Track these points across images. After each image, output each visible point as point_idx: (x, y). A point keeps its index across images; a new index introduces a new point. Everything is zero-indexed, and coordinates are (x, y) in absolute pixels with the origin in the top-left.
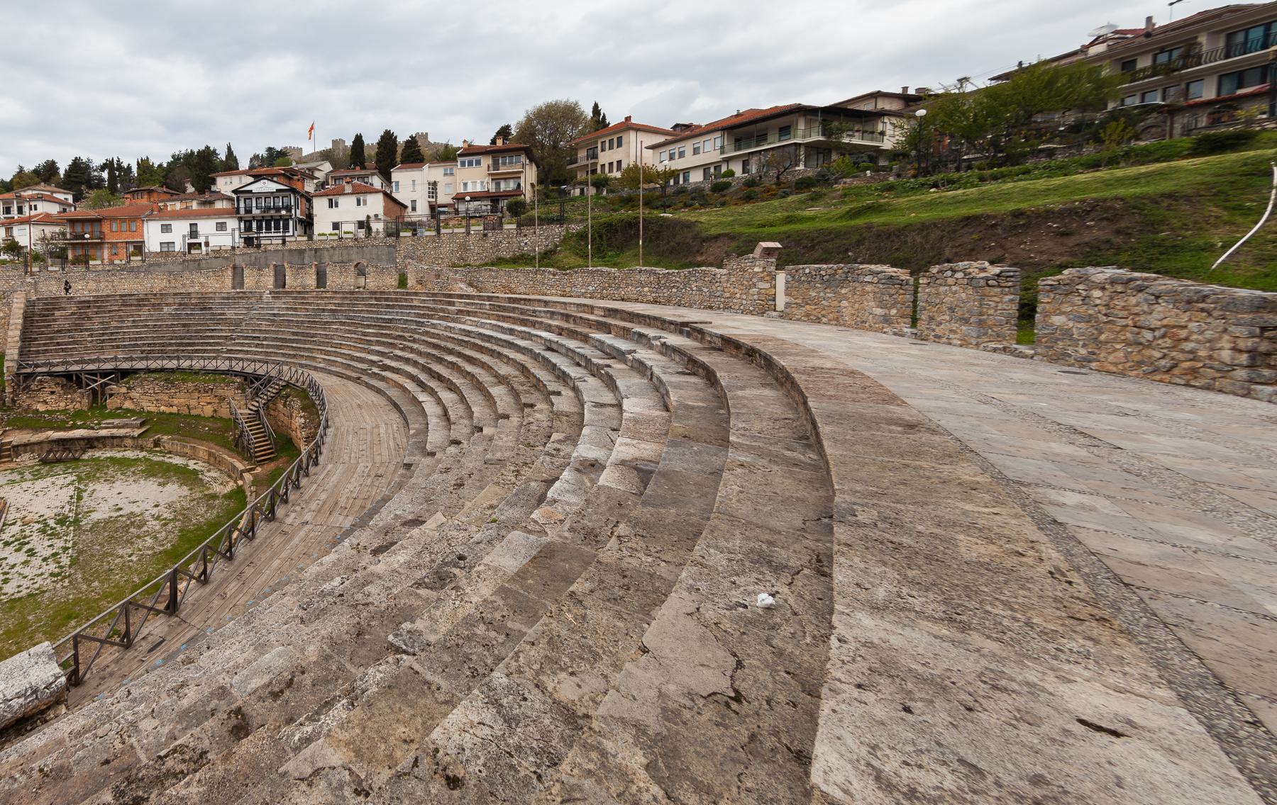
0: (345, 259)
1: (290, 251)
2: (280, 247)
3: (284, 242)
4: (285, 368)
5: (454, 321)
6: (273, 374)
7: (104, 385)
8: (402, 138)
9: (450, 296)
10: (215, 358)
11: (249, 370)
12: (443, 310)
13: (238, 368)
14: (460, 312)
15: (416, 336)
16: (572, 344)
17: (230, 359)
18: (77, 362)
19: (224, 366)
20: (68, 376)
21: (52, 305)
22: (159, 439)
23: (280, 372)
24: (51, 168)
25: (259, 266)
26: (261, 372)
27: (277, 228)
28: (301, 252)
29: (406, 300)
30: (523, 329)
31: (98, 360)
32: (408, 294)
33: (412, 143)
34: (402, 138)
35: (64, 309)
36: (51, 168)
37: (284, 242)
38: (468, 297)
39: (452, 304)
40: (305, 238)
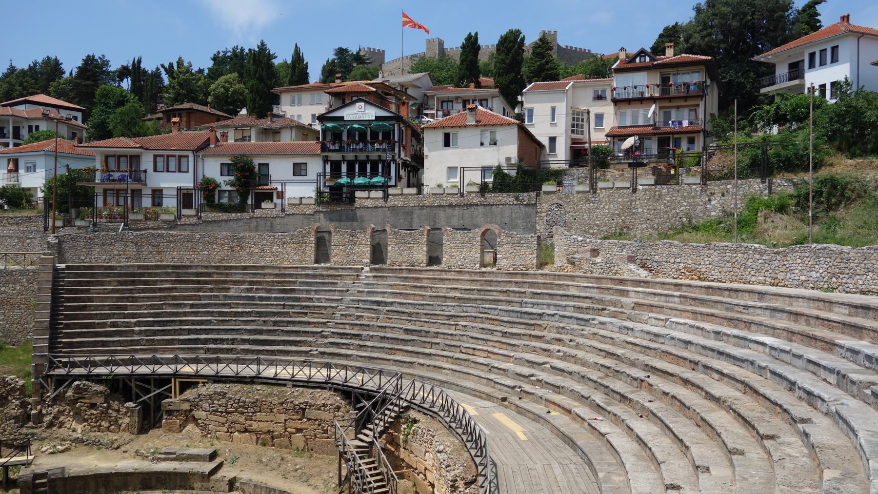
0: (467, 223)
2: (381, 203)
3: (386, 197)
5: (629, 319)
6: (390, 389)
9: (622, 282)
12: (614, 304)
15: (581, 340)
16: (812, 354)
17: (328, 366)
18: (125, 363)
19: (320, 375)
21: (89, 275)
26: (371, 385)
29: (559, 286)
30: (735, 332)
37: (386, 197)
40: (413, 191)
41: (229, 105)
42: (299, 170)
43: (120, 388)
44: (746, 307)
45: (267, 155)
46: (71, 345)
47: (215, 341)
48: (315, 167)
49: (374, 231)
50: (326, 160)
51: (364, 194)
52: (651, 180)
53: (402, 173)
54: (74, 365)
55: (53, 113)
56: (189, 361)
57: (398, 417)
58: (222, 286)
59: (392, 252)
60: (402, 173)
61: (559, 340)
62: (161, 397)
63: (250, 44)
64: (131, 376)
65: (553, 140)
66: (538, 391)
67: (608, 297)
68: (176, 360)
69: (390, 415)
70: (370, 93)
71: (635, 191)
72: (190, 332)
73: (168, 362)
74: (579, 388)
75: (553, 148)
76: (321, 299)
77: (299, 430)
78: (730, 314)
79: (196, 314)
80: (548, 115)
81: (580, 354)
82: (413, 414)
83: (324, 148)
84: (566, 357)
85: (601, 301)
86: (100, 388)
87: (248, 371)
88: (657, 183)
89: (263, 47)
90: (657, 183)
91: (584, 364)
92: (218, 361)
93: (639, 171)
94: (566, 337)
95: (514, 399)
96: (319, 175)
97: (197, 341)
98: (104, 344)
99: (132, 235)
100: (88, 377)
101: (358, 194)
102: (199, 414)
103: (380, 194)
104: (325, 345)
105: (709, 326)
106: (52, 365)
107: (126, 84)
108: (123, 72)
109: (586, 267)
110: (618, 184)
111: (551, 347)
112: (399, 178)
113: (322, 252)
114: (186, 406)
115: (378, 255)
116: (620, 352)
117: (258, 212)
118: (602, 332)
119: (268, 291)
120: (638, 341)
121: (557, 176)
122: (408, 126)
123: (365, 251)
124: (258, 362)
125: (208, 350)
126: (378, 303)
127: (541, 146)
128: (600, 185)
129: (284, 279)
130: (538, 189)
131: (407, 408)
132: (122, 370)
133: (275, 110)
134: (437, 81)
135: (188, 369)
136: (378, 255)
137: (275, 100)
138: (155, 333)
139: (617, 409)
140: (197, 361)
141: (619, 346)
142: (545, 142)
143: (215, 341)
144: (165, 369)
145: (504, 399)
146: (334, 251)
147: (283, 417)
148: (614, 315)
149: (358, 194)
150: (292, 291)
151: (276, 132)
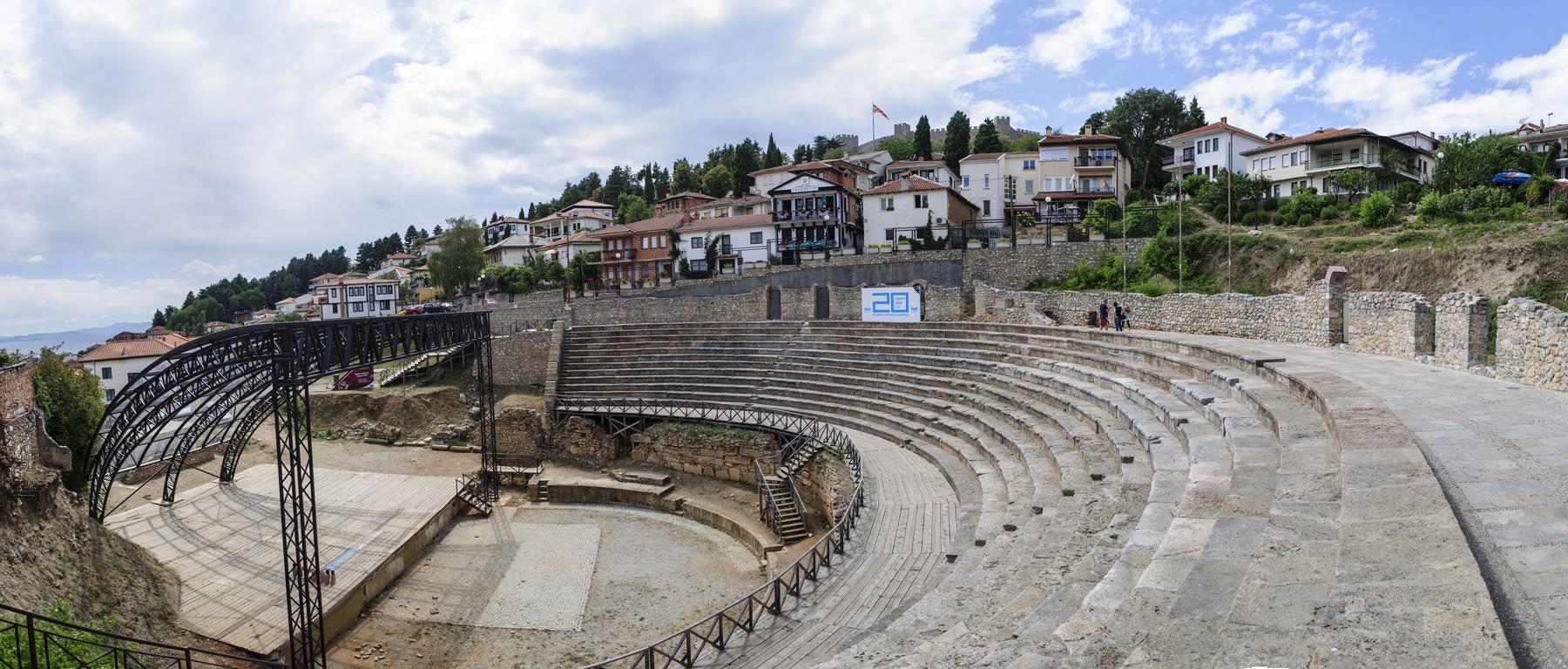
1: (835, 268)
2: (823, 264)
3: (828, 257)
4: (821, 425)
5: (1024, 364)
6: (807, 432)
7: (630, 432)
8: (976, 122)
9: (1023, 330)
10: (743, 409)
11: (780, 426)
12: (1013, 349)
13: (767, 423)
14: (1033, 351)
15: (980, 385)
17: (759, 410)
20: (596, 417)
21: (586, 335)
22: (681, 501)
23: (815, 430)
24: (594, 179)
25: (798, 286)
26: (793, 429)
27: (820, 237)
28: (847, 270)
29: (971, 335)
31: (623, 403)
32: (973, 327)
33: (988, 128)
34: (976, 122)
35: (595, 341)
36: (594, 179)
37: (828, 257)
38: (1043, 331)
39: (1024, 340)
41: (717, 189)
42: (756, 238)
43: (601, 422)
44: (1116, 350)
45: (728, 228)
46: (571, 389)
47: (676, 388)
48: (769, 234)
49: (818, 289)
50: (778, 228)
51: (808, 256)
52: (1064, 238)
53: (846, 236)
54: (570, 404)
55: (589, 213)
56: (651, 404)
57: (812, 457)
58: (684, 340)
59: (833, 306)
60: (846, 236)
61: (963, 386)
62: (630, 432)
63: (736, 142)
64: (609, 413)
65: (987, 203)
66: (938, 434)
67: (1009, 344)
68: (641, 403)
69: (805, 456)
70: (827, 169)
71: (1049, 246)
72: (657, 380)
73: (633, 404)
74: (971, 430)
75: (987, 212)
76: (764, 353)
77: (735, 465)
78: (1103, 358)
79: (662, 365)
80: (984, 181)
81: (978, 398)
82: (825, 456)
83: (775, 219)
84: (966, 401)
85: (1003, 348)
86: (585, 422)
87: (695, 413)
88: (1070, 240)
89: (748, 141)
90: (1070, 240)
91: (982, 408)
92: (671, 404)
93: (1054, 230)
94: (967, 383)
95: (917, 442)
96: (769, 242)
97: (663, 388)
98: (594, 388)
99: (622, 301)
100: (580, 413)
101: (803, 257)
102: (658, 446)
103: (822, 256)
104: (764, 392)
105: (1085, 369)
106: (557, 404)
107: (643, 183)
108: (640, 176)
109: (1003, 316)
110: (1035, 241)
111: (955, 392)
112: (844, 242)
113: (774, 311)
114: (648, 440)
115: (822, 310)
116: (1009, 395)
117: (719, 278)
118: (999, 377)
119: (722, 345)
120: (1026, 385)
121: (985, 238)
122: (850, 195)
123: (809, 305)
124: (703, 406)
125: (669, 396)
126: (814, 354)
127: (977, 209)
128: (1019, 242)
129: (736, 337)
130: (965, 248)
131: (821, 450)
132: (602, 409)
133: (752, 189)
134: (897, 156)
135: (649, 411)
136: (822, 310)
137: (752, 182)
138: (630, 380)
139: (994, 449)
140: (656, 404)
141: (1013, 390)
142: (981, 206)
143: (676, 388)
144: (633, 410)
145: (908, 442)
146: (784, 308)
147: (721, 453)
148: (1012, 361)
149: (803, 257)
150: (741, 344)
151: (749, 209)
